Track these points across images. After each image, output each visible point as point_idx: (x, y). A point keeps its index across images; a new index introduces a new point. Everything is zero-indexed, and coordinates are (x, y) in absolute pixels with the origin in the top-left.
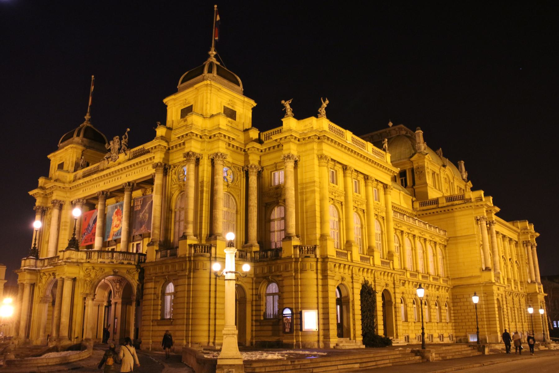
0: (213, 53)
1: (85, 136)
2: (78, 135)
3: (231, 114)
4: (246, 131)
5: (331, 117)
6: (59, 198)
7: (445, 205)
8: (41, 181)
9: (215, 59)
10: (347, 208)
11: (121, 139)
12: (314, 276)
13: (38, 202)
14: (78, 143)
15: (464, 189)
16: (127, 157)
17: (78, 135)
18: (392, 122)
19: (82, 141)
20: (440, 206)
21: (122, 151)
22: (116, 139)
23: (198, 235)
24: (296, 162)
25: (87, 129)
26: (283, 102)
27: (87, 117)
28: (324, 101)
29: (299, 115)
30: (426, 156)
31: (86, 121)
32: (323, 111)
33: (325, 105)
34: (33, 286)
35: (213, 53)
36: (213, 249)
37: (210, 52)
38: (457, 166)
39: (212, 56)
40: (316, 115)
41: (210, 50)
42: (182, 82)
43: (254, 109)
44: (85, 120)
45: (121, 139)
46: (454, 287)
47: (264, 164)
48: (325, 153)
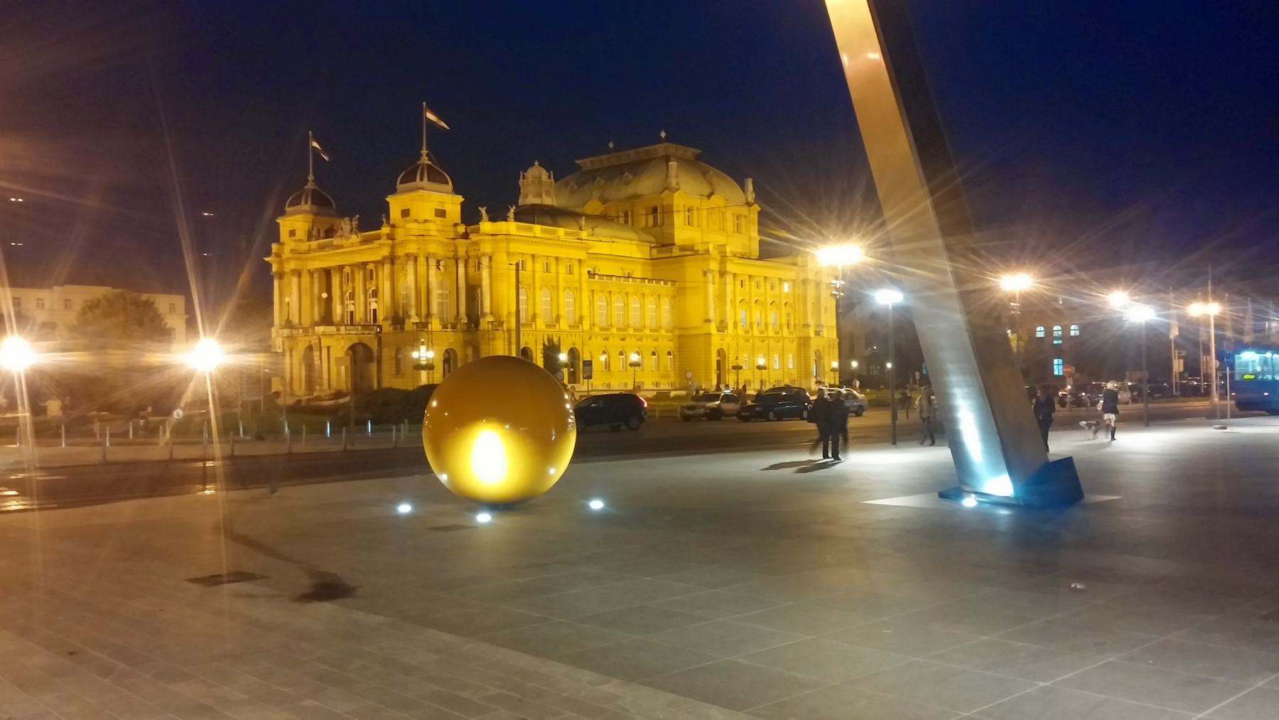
0: (424, 152)
1: (312, 203)
2: (306, 203)
3: (441, 213)
4: (456, 225)
5: (516, 220)
6: (298, 268)
7: (677, 254)
8: (274, 247)
9: (427, 158)
10: (534, 289)
11: (351, 221)
12: (502, 342)
13: (274, 268)
14: (306, 212)
15: (747, 214)
16: (359, 240)
17: (306, 203)
18: (665, 132)
19: (311, 208)
20: (673, 255)
21: (353, 232)
22: (347, 219)
23: (418, 314)
24: (491, 258)
25: (314, 191)
26: (480, 208)
27: (311, 177)
28: (512, 207)
29: (493, 219)
30: (675, 194)
31: (309, 183)
32: (511, 214)
33: (512, 210)
34: (291, 350)
35: (424, 152)
36: (430, 325)
37: (422, 152)
38: (743, 187)
39: (424, 155)
40: (505, 219)
41: (422, 149)
42: (400, 183)
43: (462, 204)
44: (308, 180)
45: (351, 221)
46: (680, 336)
47: (470, 254)
48: (511, 250)
